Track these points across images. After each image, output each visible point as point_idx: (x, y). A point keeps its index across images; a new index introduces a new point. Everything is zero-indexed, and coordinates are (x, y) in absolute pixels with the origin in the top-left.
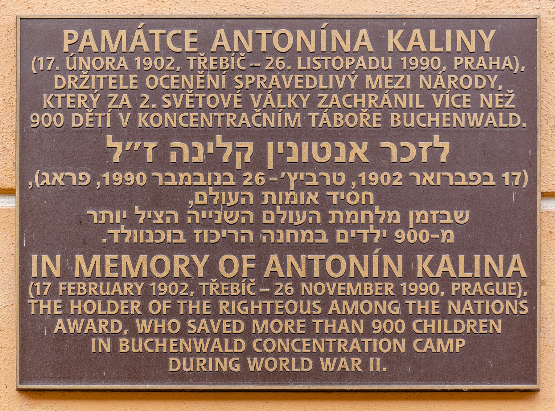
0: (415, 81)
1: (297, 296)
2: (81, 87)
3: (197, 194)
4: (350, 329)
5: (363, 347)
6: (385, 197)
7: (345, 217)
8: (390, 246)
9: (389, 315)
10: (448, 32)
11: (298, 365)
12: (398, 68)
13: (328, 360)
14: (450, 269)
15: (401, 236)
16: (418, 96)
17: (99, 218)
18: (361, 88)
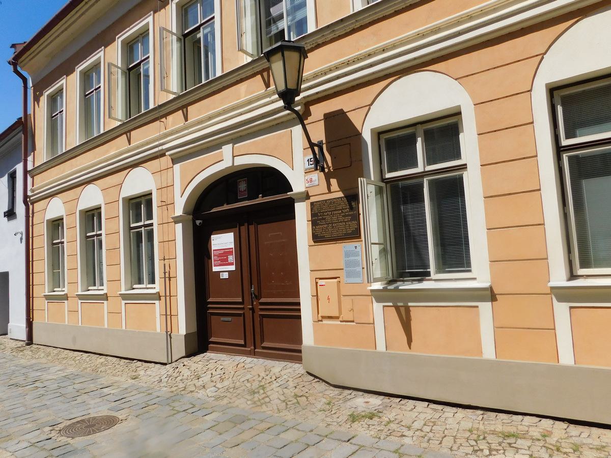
6: (343, 216)
8: (344, 222)
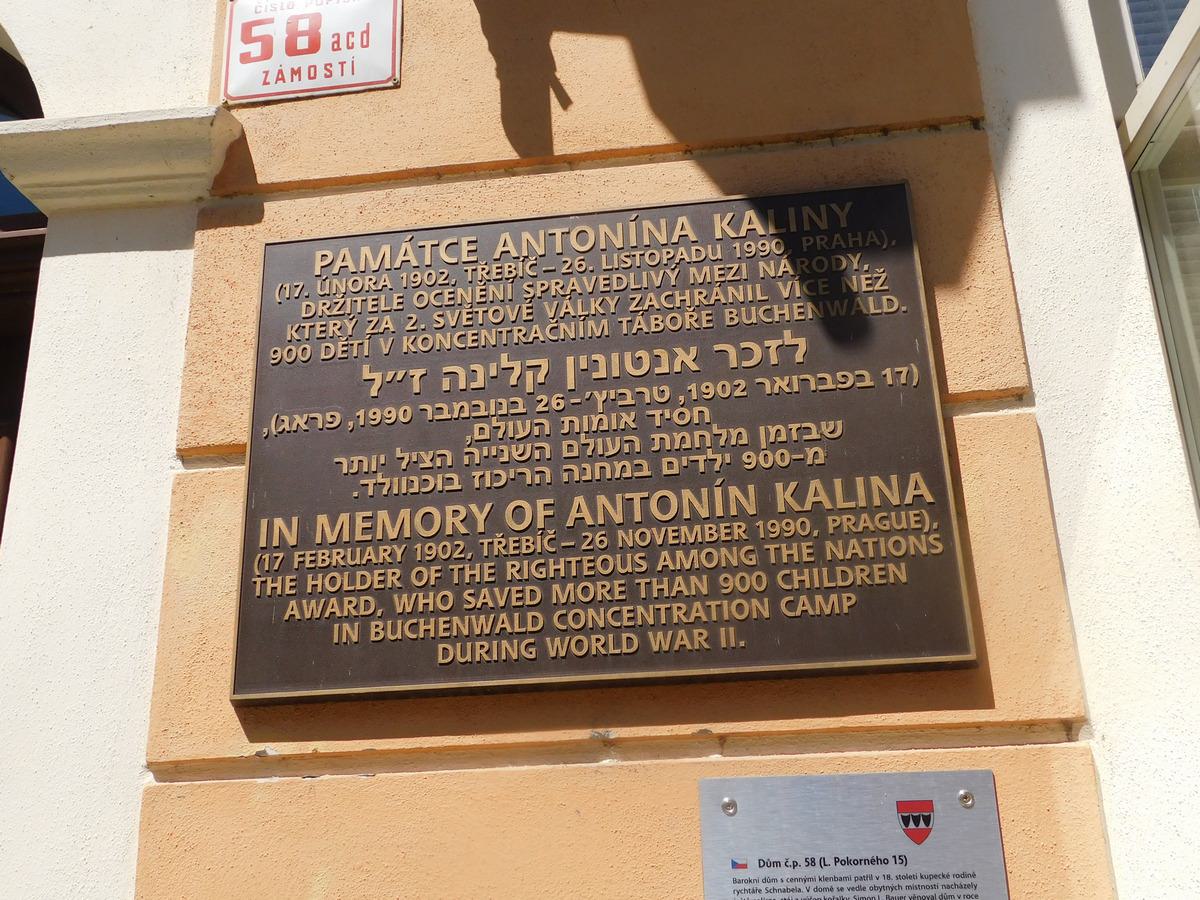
0: (753, 270)
1: (611, 549)
2: (335, 312)
3: (477, 426)
4: (689, 589)
5: (708, 614)
6: (725, 411)
7: (672, 442)
8: (736, 474)
9: (741, 567)
10: (792, 211)
11: (617, 644)
12: (730, 256)
13: (660, 634)
14: (823, 498)
15: (750, 459)
16: (758, 286)
17: (350, 466)
18: (684, 284)
